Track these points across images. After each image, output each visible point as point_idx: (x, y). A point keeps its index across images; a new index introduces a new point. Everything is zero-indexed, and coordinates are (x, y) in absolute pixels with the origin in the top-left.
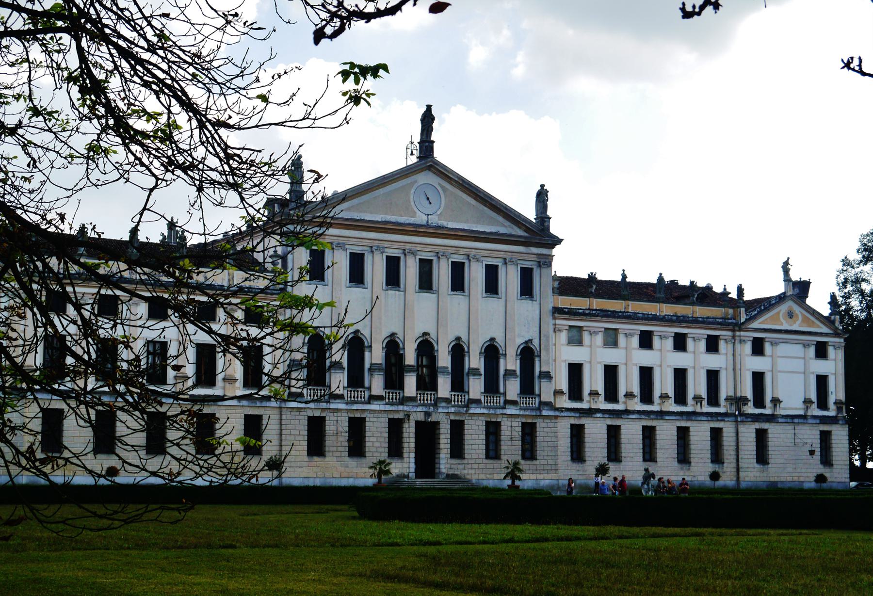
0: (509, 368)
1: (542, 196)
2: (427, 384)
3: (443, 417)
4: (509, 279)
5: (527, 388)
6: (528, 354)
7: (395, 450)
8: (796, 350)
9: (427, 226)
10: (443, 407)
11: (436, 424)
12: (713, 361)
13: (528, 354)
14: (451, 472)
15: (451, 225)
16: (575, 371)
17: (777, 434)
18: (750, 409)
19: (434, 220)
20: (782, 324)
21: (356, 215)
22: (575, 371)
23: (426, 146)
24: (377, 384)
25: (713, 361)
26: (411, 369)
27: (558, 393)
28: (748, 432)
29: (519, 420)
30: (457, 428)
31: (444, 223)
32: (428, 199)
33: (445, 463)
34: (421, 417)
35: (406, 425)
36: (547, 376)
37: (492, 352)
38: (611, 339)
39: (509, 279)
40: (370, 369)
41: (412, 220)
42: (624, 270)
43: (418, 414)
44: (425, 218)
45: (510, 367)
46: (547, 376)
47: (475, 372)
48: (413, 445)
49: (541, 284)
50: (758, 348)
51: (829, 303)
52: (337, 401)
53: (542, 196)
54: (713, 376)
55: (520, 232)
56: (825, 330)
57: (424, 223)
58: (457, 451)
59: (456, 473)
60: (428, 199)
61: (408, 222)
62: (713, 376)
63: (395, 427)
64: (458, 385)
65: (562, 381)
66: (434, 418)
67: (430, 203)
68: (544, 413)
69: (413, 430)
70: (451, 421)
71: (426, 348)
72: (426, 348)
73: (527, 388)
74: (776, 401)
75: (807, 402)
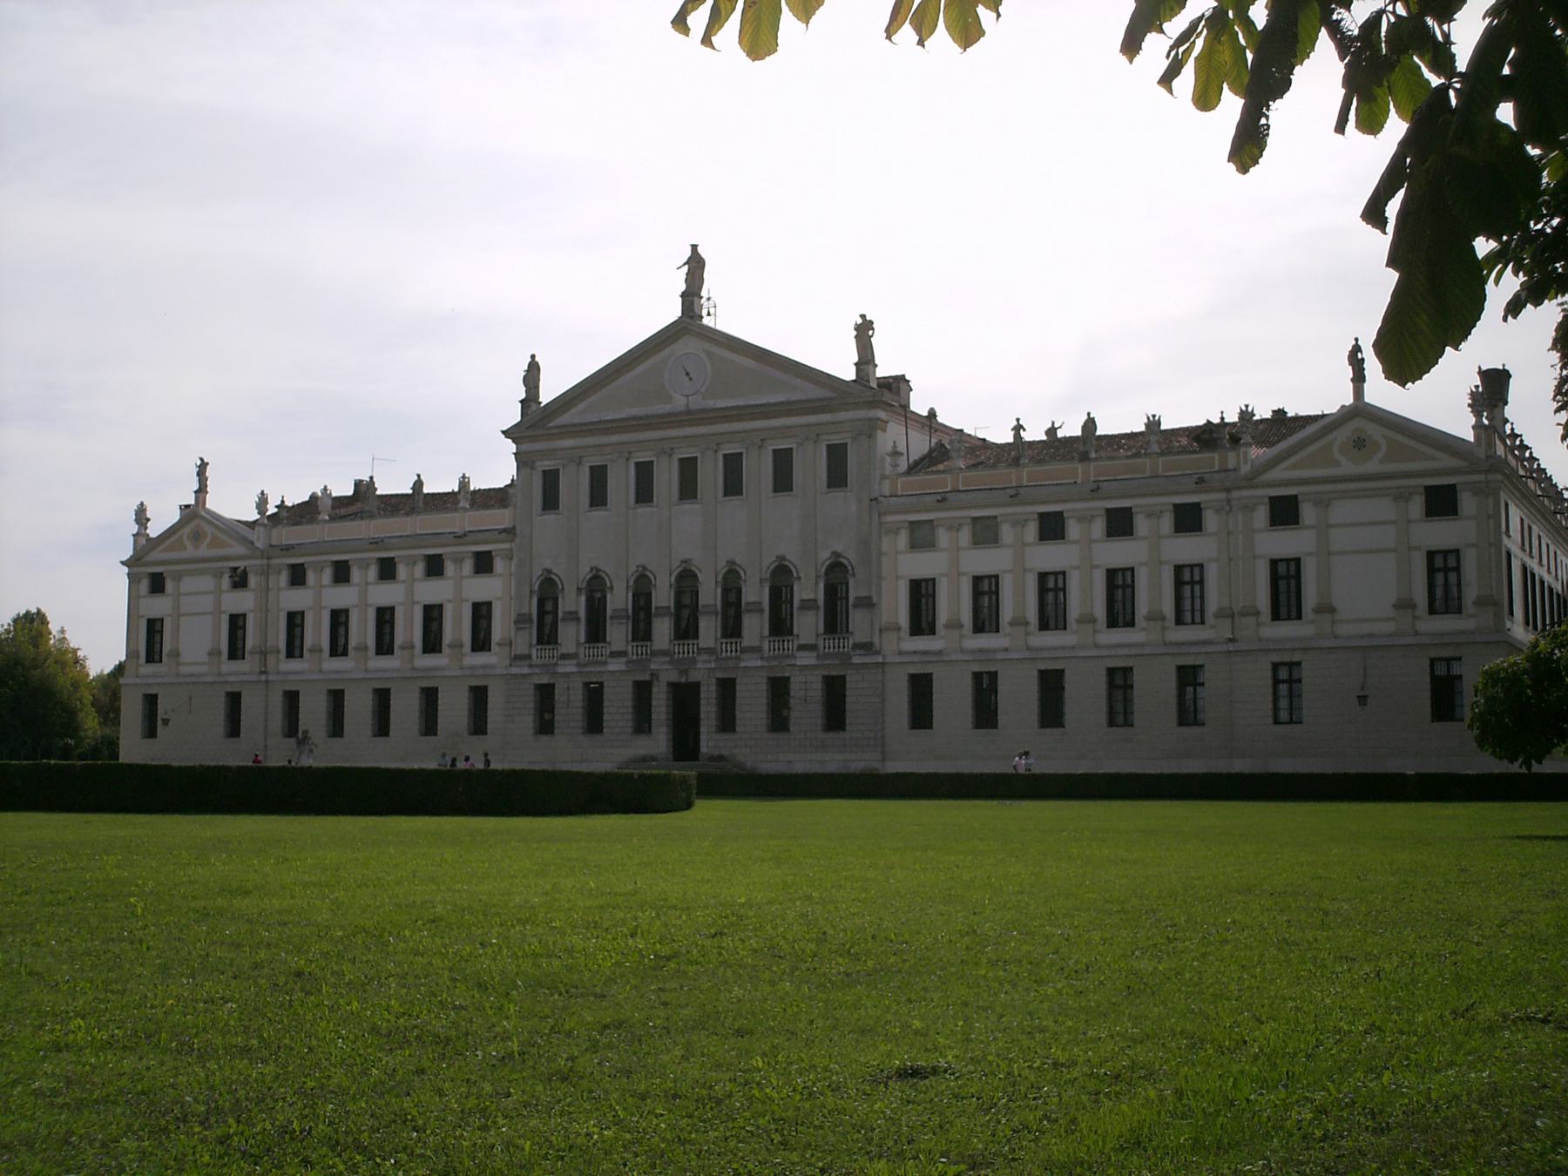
0: (806, 597)
1: (864, 330)
2: (686, 630)
3: (704, 673)
5: (834, 623)
7: (642, 724)
8: (1382, 508)
9: (689, 412)
10: (704, 662)
11: (695, 687)
12: (1188, 549)
14: (716, 752)
15: (720, 404)
16: (922, 593)
19: (696, 403)
20: (1337, 464)
21: (593, 417)
22: (922, 593)
23: (691, 296)
24: (618, 634)
25: (1188, 549)
29: (818, 672)
30: (727, 688)
31: (711, 403)
32: (687, 374)
33: (710, 740)
34: (674, 677)
35: (655, 690)
36: (867, 603)
38: (985, 533)
40: (611, 617)
41: (667, 408)
42: (1018, 420)
43: (669, 675)
44: (683, 400)
45: (808, 595)
47: (756, 608)
48: (663, 717)
51: (1469, 405)
52: (567, 662)
53: (864, 330)
57: (683, 409)
58: (727, 722)
59: (723, 752)
60: (687, 374)
61: (661, 411)
63: (642, 691)
64: (732, 629)
65: (898, 607)
66: (694, 676)
67: (691, 379)
68: (856, 660)
69: (663, 696)
70: (718, 679)
73: (834, 623)
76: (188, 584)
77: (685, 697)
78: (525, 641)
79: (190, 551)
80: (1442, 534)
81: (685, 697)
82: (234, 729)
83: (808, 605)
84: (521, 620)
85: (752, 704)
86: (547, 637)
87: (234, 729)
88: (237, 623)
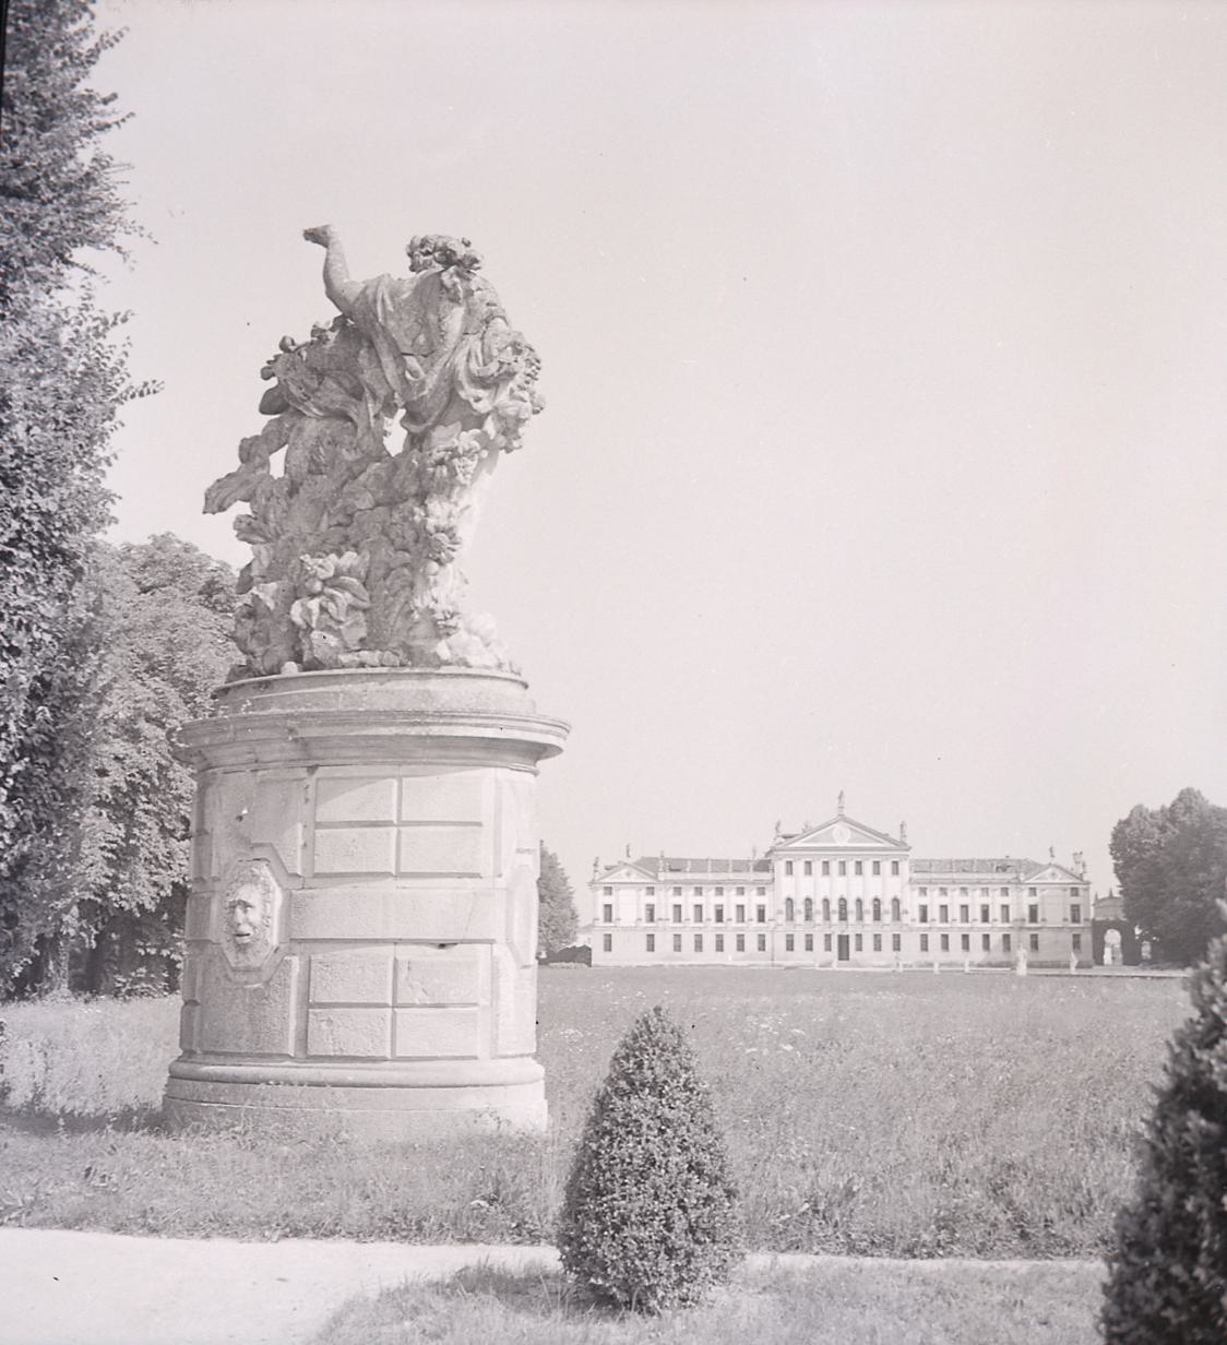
3: (851, 932)
4: (886, 867)
6: (896, 901)
7: (828, 948)
13: (896, 901)
17: (1044, 938)
18: (1028, 925)
22: (924, 910)
26: (834, 912)
27: (913, 920)
28: (1026, 936)
30: (859, 936)
36: (906, 912)
37: (877, 901)
39: (886, 867)
46: (906, 912)
49: (904, 867)
50: (1033, 891)
54: (1005, 908)
55: (892, 845)
56: (1076, 881)
58: (859, 948)
62: (1005, 908)
63: (828, 937)
64: (860, 918)
65: (917, 915)
71: (843, 903)
72: (843, 903)
74: (1044, 920)
75: (1065, 920)
76: (621, 892)
77: (844, 940)
78: (782, 918)
79: (626, 880)
80: (1075, 900)
81: (844, 940)
82: (651, 948)
83: (887, 912)
84: (780, 912)
85: (868, 943)
86: (790, 917)
87: (651, 948)
88: (651, 910)
